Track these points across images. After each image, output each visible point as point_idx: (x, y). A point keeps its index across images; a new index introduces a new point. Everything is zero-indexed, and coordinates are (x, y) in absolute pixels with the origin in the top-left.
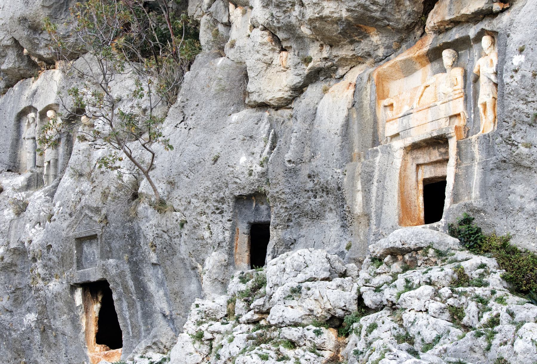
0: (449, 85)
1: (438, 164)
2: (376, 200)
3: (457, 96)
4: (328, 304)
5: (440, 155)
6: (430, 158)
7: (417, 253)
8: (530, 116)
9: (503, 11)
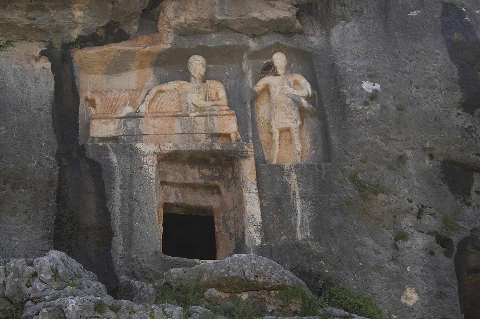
0: (202, 96)
1: (188, 190)
2: (122, 212)
3: (225, 112)
5: (201, 178)
6: (185, 178)
7: (269, 294)
8: (391, 156)
9: (301, 32)
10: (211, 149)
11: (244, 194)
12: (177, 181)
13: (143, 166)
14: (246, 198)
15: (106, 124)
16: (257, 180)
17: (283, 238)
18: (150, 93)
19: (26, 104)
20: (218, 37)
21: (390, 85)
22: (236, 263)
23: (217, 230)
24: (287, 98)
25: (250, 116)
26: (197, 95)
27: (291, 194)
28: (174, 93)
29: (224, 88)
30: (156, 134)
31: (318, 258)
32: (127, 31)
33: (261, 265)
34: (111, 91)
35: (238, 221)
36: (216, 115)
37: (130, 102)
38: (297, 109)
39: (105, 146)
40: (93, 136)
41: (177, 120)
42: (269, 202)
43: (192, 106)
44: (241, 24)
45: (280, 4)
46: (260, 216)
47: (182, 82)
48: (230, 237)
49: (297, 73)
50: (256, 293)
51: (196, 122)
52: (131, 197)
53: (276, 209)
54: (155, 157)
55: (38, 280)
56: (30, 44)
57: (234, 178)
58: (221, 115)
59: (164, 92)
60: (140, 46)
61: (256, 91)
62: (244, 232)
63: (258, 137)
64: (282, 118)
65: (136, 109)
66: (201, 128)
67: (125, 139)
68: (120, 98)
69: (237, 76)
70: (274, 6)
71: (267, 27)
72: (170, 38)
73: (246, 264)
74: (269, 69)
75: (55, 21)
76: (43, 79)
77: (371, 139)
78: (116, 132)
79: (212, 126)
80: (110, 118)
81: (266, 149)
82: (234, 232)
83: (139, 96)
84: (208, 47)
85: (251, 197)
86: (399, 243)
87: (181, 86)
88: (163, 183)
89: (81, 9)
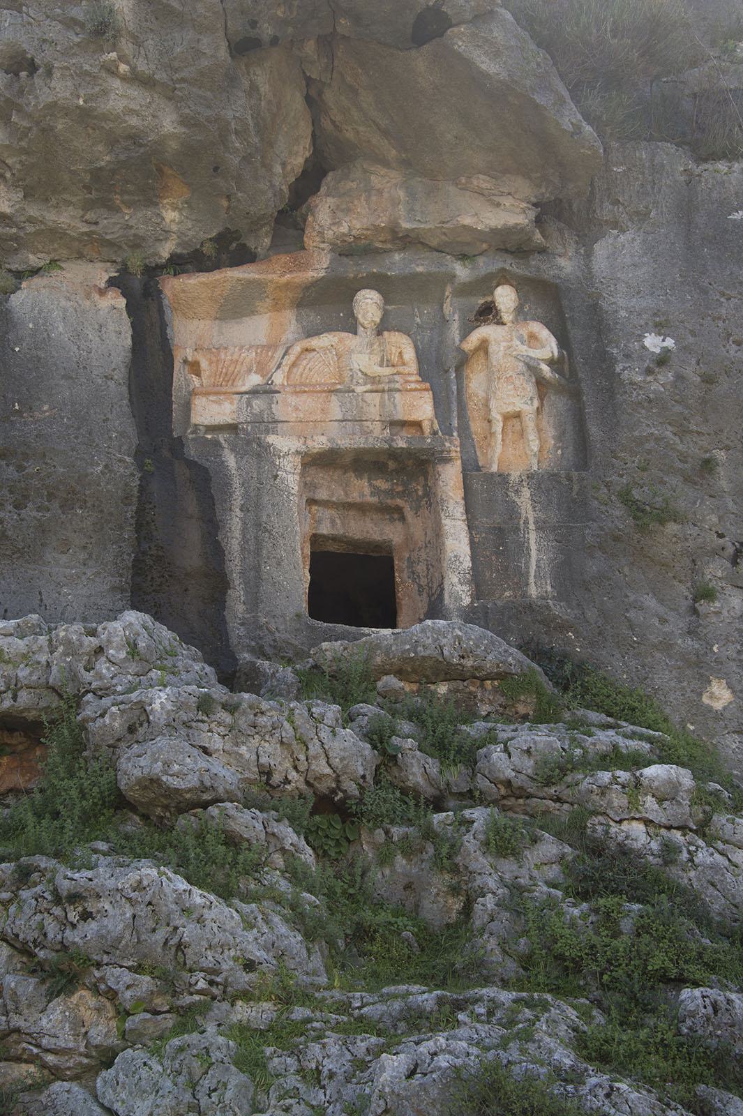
0: (377, 358)
1: (351, 513)
2: (243, 549)
3: (413, 386)
4: (323, 762)
5: (372, 494)
6: (346, 494)
7: (482, 686)
8: (690, 460)
9: (542, 251)
10: (390, 446)
11: (443, 522)
12: (334, 499)
13: (279, 473)
14: (446, 528)
15: (218, 403)
16: (465, 498)
17: (507, 594)
18: (290, 351)
19: (85, 368)
20: (404, 259)
21: (691, 339)
22: (429, 634)
23: (398, 579)
24: (517, 363)
25: (455, 392)
26: (367, 356)
27: (522, 522)
28: (331, 352)
29: (412, 345)
30: (301, 421)
31: (563, 627)
32: (253, 247)
33: (469, 639)
34: (226, 348)
35: (433, 566)
36: (400, 391)
37: (257, 367)
38: (534, 380)
39: (216, 441)
40: (197, 423)
41: (334, 397)
42: (484, 535)
43: (360, 374)
44: (443, 237)
45: (508, 202)
46: (468, 558)
47: (344, 335)
48: (419, 591)
49: (535, 320)
50: (461, 685)
51: (366, 402)
52: (258, 525)
53: (495, 547)
54: (298, 459)
55: (104, 659)
56: (91, 265)
57: (427, 494)
58: (407, 390)
59: (314, 350)
60: (274, 273)
61: (466, 350)
62: (442, 583)
63: (468, 428)
64: (508, 395)
65: (267, 378)
66: (373, 411)
67: (249, 428)
68: (241, 360)
69: (435, 324)
70: (498, 205)
71: (486, 242)
72: (324, 259)
73: (446, 637)
74: (488, 313)
75: (132, 227)
76: (112, 327)
77: (656, 432)
78: (234, 416)
79: (392, 409)
80: (225, 393)
81: (480, 447)
82: (426, 583)
83: (272, 357)
84: (387, 275)
85: (454, 526)
86: (701, 605)
87: (341, 341)
88: (312, 502)
89: (175, 208)
